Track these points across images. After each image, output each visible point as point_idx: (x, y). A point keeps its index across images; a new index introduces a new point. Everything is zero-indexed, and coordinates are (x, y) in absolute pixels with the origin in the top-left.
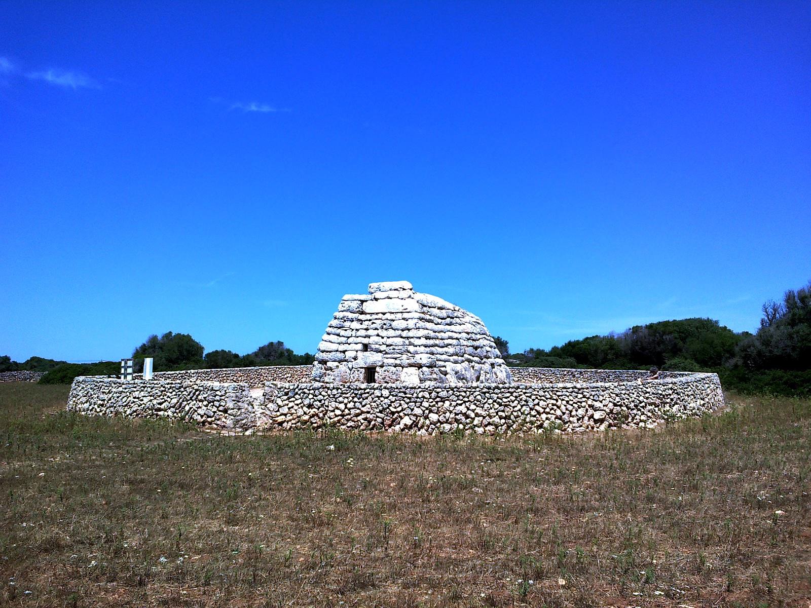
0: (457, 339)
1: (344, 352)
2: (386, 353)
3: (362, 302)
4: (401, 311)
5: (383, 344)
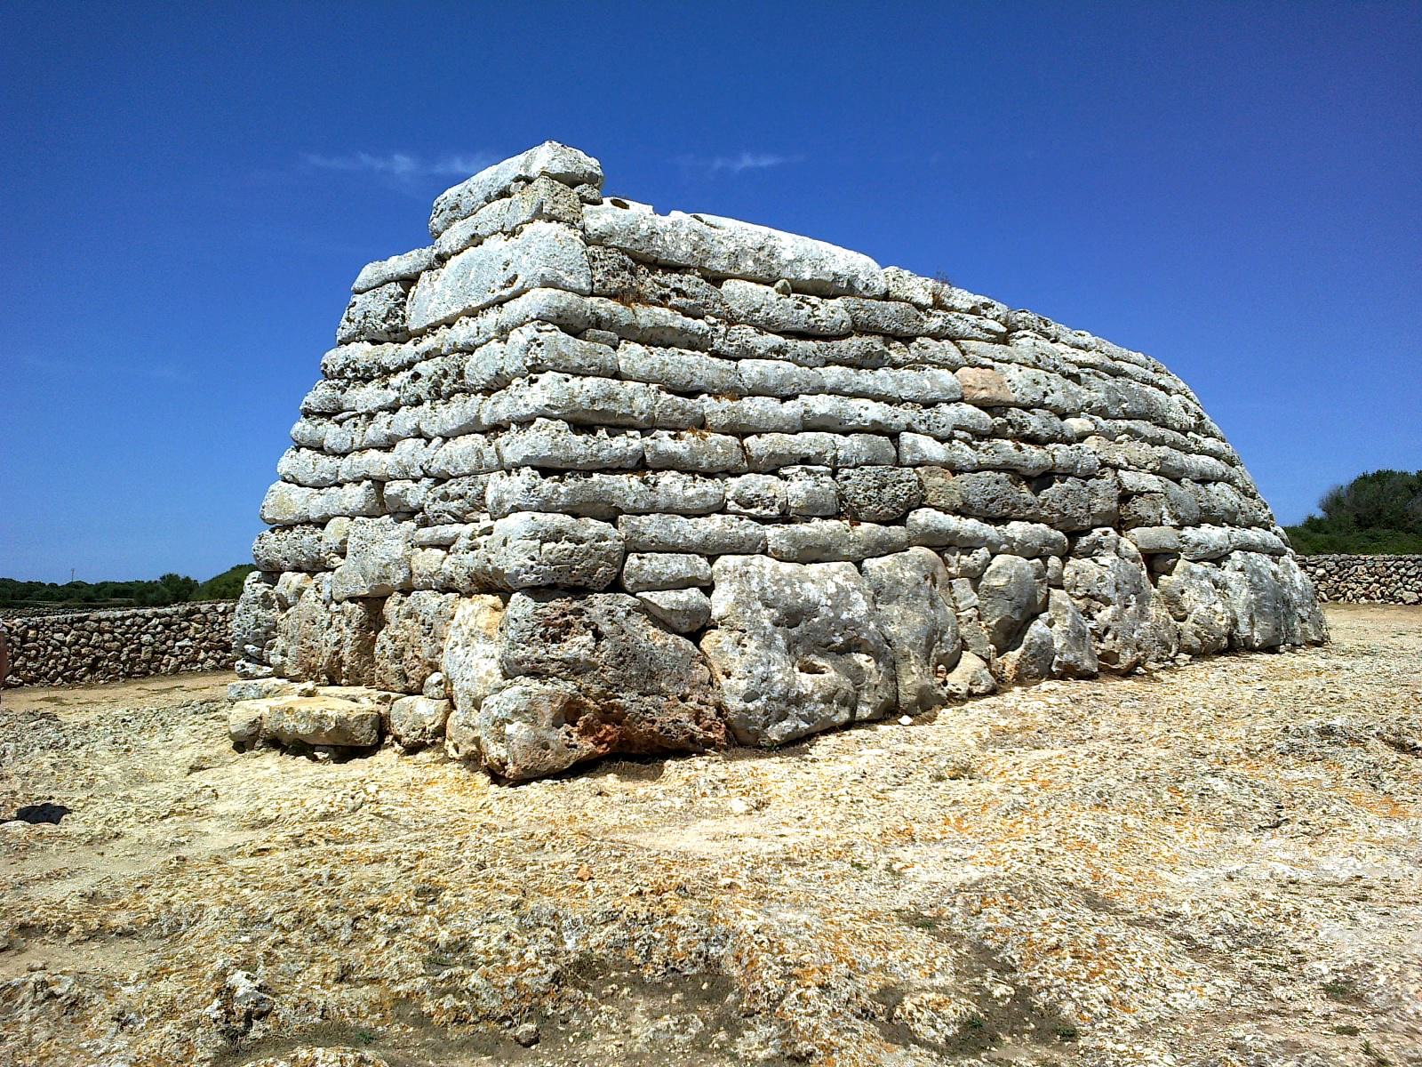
0: (877, 429)
2: (425, 523)
3: (409, 281)
5: (426, 475)
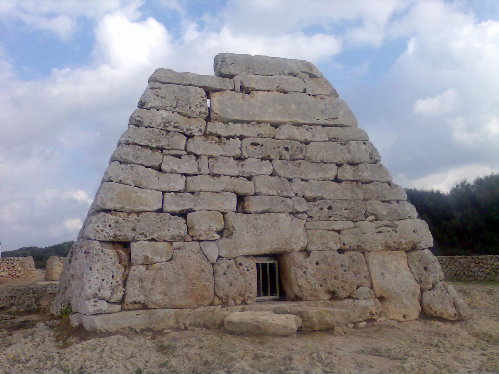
1: (183, 214)
4: (323, 122)
